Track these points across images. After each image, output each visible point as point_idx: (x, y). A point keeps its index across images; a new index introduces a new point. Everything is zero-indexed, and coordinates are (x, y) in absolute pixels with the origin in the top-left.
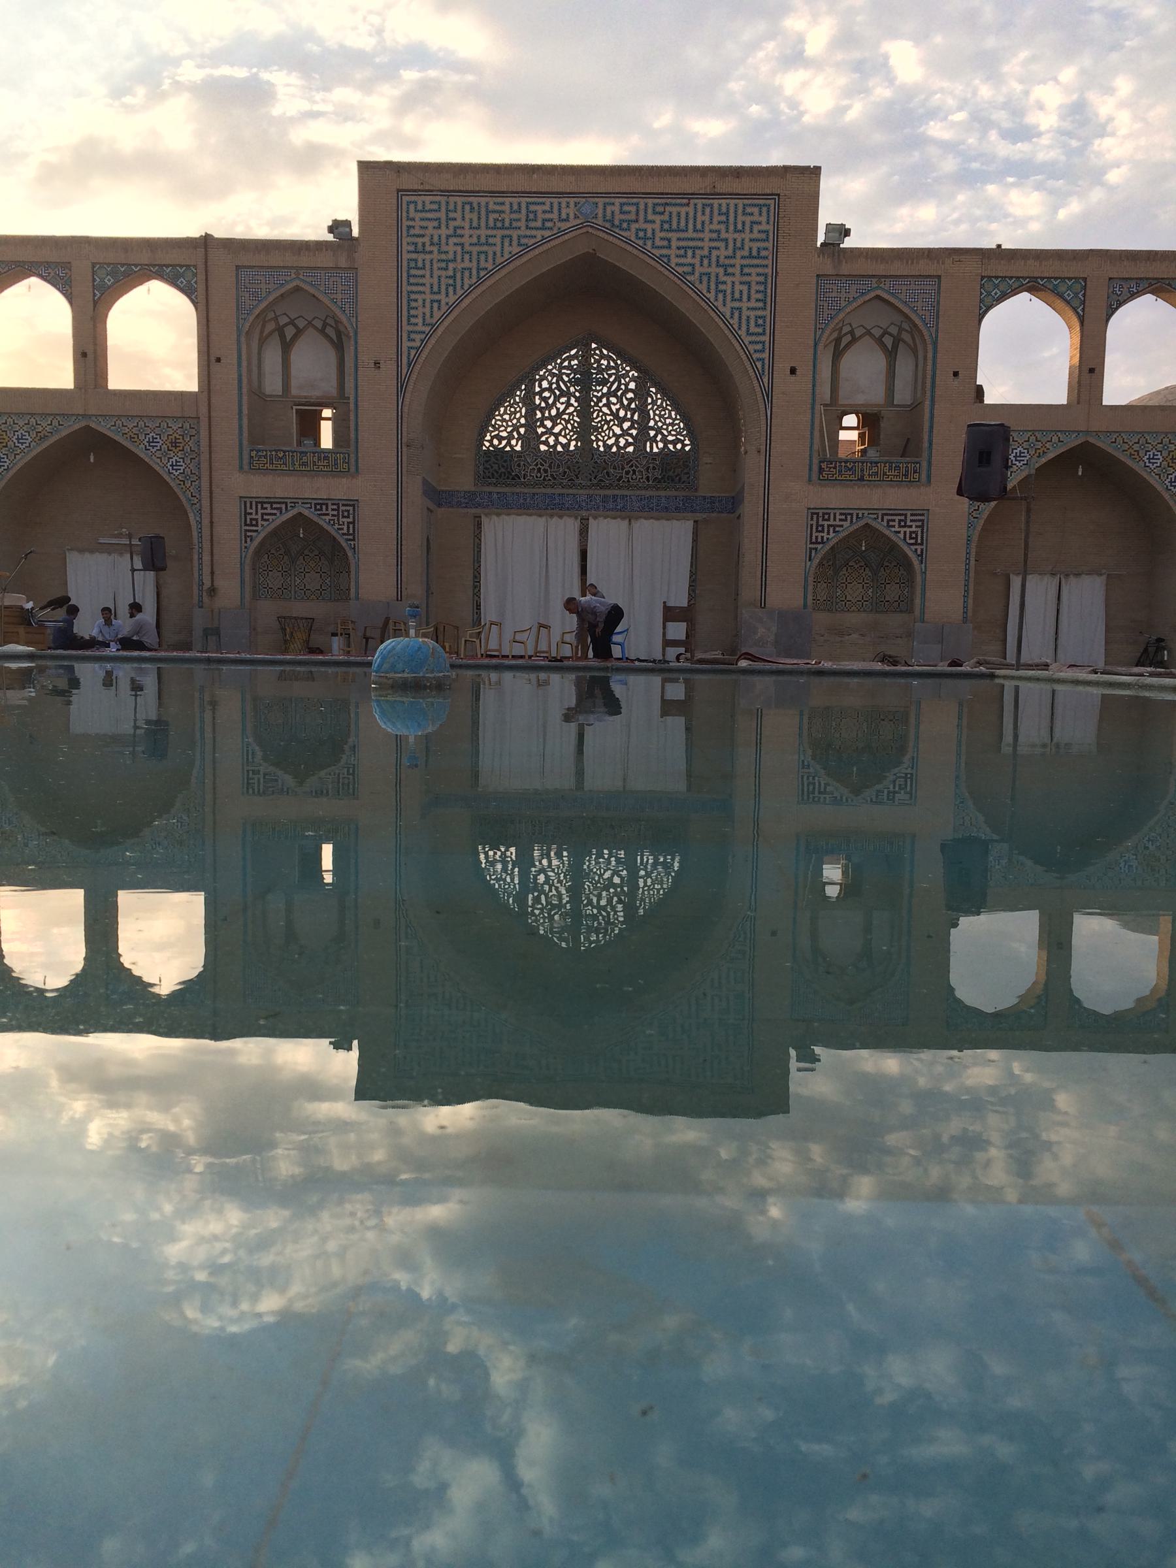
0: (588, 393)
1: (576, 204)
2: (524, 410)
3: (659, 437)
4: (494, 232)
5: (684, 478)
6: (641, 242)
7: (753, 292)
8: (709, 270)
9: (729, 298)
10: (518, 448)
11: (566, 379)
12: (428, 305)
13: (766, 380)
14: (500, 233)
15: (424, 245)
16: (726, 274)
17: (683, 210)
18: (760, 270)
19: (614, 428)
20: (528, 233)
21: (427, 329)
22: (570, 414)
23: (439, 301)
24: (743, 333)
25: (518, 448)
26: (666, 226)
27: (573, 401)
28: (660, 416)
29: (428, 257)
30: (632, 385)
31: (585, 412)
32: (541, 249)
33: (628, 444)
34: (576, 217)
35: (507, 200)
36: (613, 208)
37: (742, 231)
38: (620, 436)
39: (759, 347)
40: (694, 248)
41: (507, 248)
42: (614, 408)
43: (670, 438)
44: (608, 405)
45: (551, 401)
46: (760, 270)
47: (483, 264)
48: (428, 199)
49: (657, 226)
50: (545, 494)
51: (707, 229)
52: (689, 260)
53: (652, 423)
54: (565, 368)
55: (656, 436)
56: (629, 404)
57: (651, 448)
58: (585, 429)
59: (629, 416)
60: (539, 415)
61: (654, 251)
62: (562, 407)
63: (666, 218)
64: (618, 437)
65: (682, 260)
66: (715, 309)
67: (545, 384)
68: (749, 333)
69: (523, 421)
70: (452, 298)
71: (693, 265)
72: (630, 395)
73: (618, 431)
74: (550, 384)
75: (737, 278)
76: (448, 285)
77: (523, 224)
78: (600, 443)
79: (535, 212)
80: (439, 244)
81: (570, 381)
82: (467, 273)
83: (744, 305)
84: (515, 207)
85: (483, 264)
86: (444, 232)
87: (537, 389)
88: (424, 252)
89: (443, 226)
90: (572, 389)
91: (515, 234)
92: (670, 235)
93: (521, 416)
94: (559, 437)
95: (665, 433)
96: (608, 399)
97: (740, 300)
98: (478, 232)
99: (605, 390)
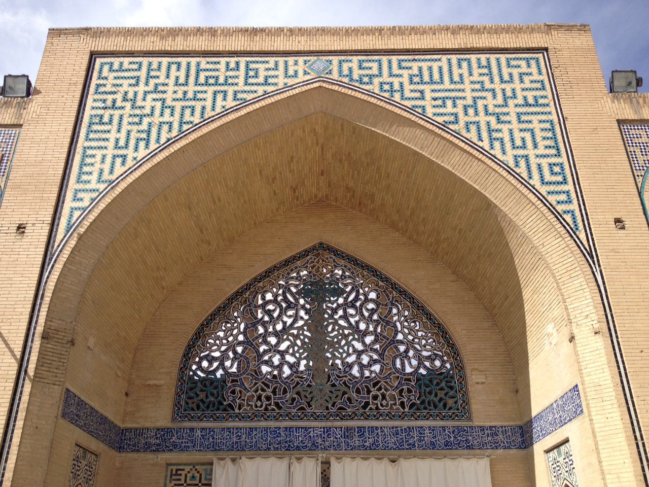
0: (320, 306)
1: (305, 62)
2: (242, 326)
3: (411, 353)
4: (205, 88)
5: (450, 402)
6: (387, 95)
7: (538, 139)
8: (477, 119)
9: (508, 146)
10: (234, 370)
11: (294, 290)
12: (109, 160)
13: (582, 236)
14: (211, 90)
15: (114, 101)
16: (499, 121)
17: (435, 66)
18: (544, 117)
19: (354, 343)
20: (247, 88)
21: (102, 187)
22: (299, 328)
23: (124, 157)
24: (536, 181)
25: (234, 370)
26: (416, 79)
27: (302, 313)
28: (410, 329)
29: (117, 113)
30: (373, 295)
31: (317, 323)
32: (263, 103)
33: (373, 362)
34: (305, 73)
35: (223, 60)
36: (350, 65)
37: (511, 80)
38: (362, 352)
39: (563, 197)
40: (454, 100)
41: (219, 102)
42: (352, 320)
43: (425, 354)
44: (345, 317)
45: (276, 315)
46: (544, 117)
47: (187, 117)
48: (126, 61)
49: (405, 80)
50: (266, 429)
51: (467, 80)
52: (449, 108)
53: (400, 337)
54: (292, 278)
55: (407, 351)
56: (371, 316)
57: (403, 364)
58: (317, 345)
59: (371, 328)
60: (261, 330)
61: (403, 102)
62: (289, 321)
63: (416, 72)
64: (359, 353)
65: (441, 110)
66: (493, 158)
67: (269, 296)
68: (543, 182)
69: (241, 338)
70: (142, 152)
71: (456, 115)
72: (371, 306)
73: (359, 346)
74: (276, 296)
75: (515, 125)
76: (138, 140)
77: (241, 81)
78: (338, 362)
79: (257, 71)
80: (141, 117)
81: (299, 293)
82: (165, 128)
83: (531, 152)
84: (232, 65)
85: (187, 117)
86: (142, 88)
87: (260, 302)
88: (114, 107)
89: (142, 84)
90: (302, 301)
91: (230, 90)
92: (421, 87)
93: (239, 333)
94: (286, 358)
95: (418, 347)
96: (345, 311)
97: (524, 147)
98: (185, 88)
99: (341, 301)
